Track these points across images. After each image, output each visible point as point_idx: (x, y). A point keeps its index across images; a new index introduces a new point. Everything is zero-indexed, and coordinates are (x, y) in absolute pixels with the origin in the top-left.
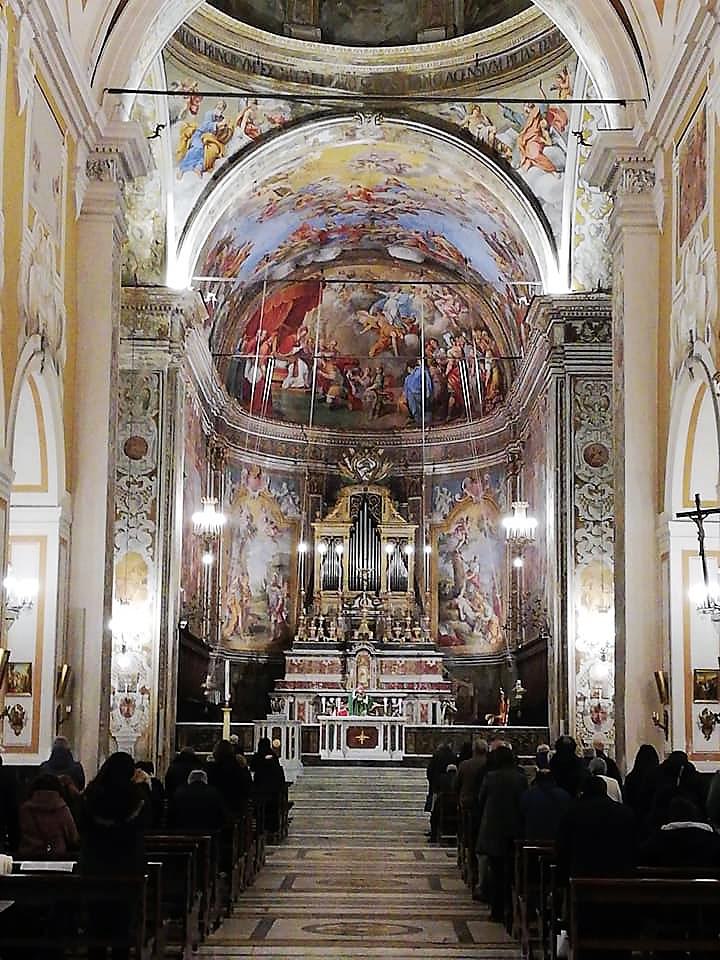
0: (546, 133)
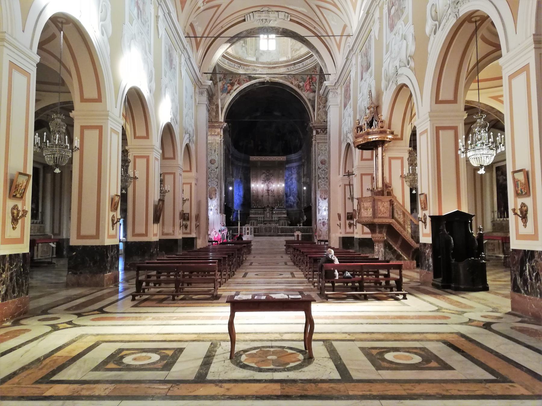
0: (311, 83)
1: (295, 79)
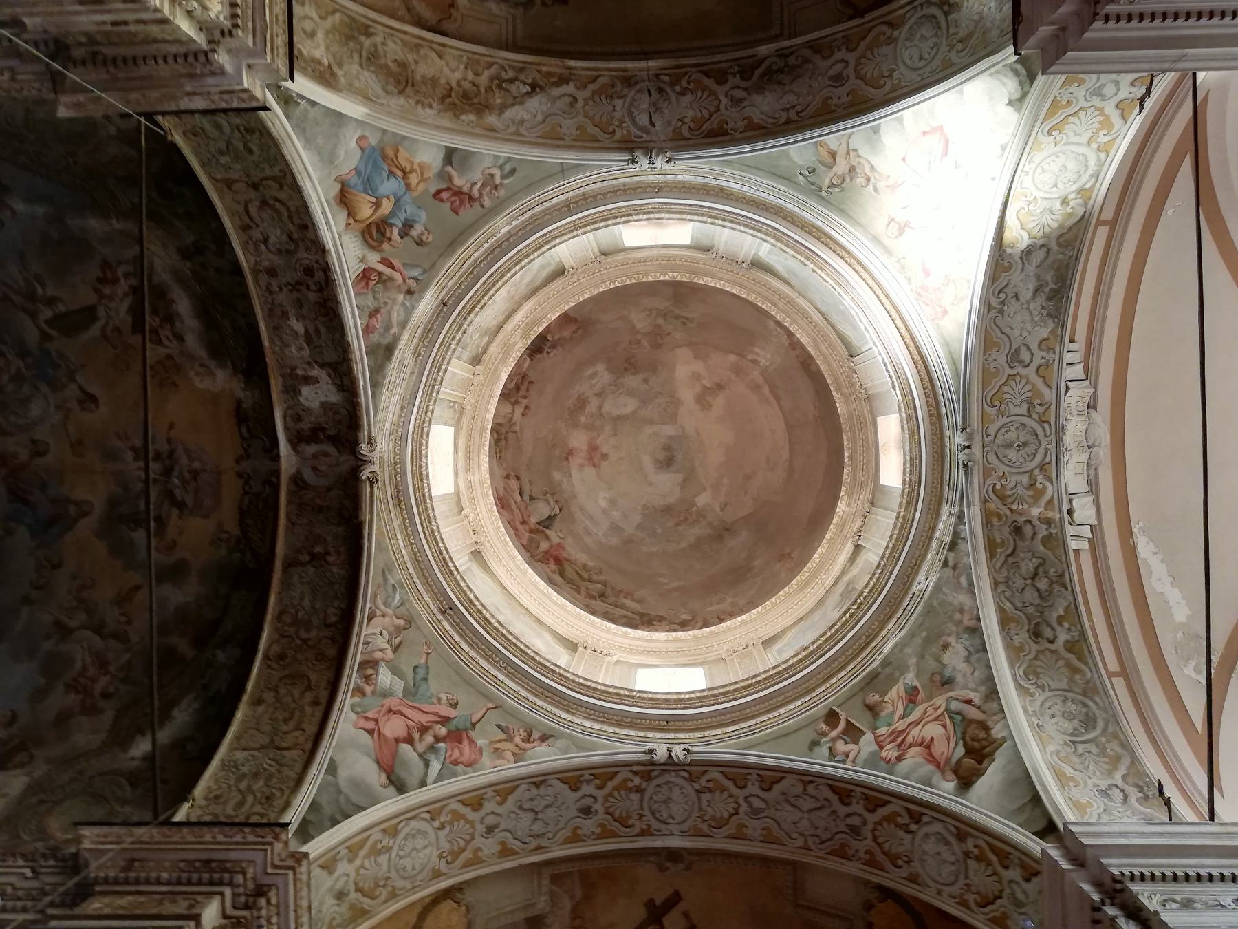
0: (429, 739)
1: (398, 630)
